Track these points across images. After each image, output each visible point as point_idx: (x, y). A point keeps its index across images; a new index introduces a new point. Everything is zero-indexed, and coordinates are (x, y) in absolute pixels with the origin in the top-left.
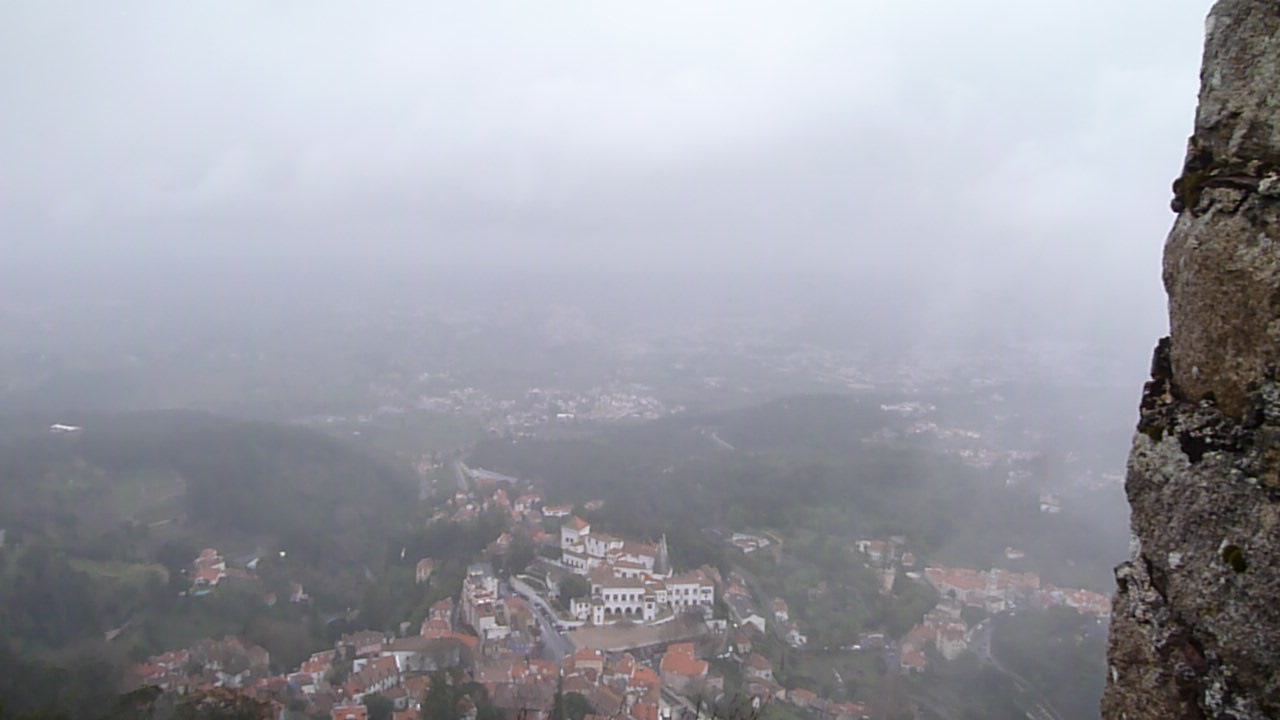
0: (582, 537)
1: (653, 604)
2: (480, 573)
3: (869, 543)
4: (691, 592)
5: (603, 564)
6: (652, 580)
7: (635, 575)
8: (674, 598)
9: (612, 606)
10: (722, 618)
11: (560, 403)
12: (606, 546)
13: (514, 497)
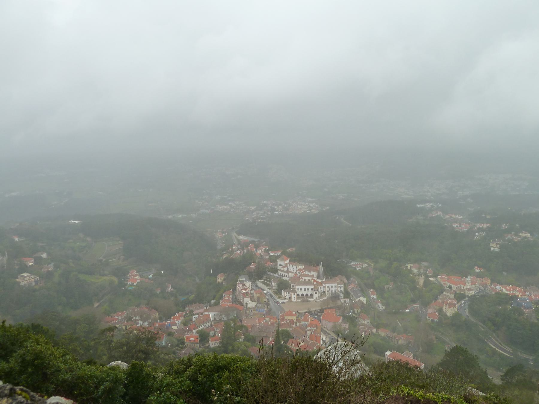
0: (286, 264)
2: (244, 279)
4: (334, 287)
7: (309, 280)
8: (327, 289)
10: (347, 298)
11: (276, 207)
13: (257, 247)
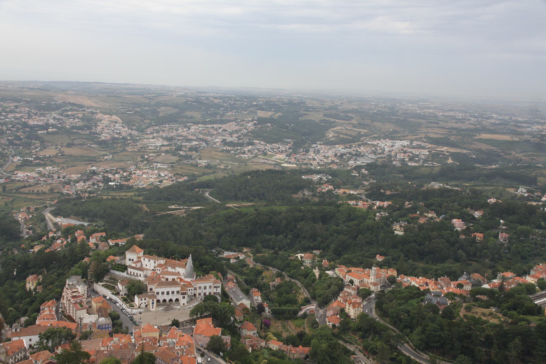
0: (139, 258)
1: (186, 296)
3: (303, 255)
4: (208, 288)
5: (154, 273)
6: (185, 282)
7: (174, 280)
8: (198, 291)
9: (161, 298)
11: (110, 176)
12: (155, 262)
13: (88, 235)
